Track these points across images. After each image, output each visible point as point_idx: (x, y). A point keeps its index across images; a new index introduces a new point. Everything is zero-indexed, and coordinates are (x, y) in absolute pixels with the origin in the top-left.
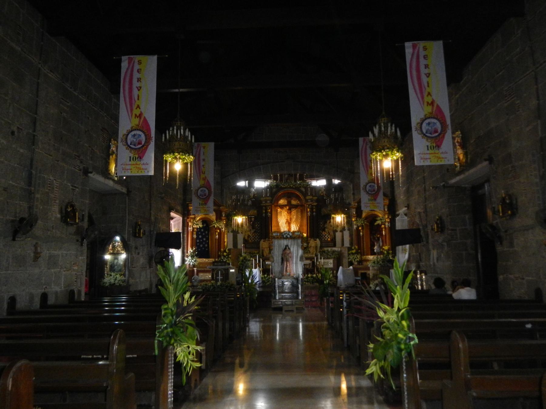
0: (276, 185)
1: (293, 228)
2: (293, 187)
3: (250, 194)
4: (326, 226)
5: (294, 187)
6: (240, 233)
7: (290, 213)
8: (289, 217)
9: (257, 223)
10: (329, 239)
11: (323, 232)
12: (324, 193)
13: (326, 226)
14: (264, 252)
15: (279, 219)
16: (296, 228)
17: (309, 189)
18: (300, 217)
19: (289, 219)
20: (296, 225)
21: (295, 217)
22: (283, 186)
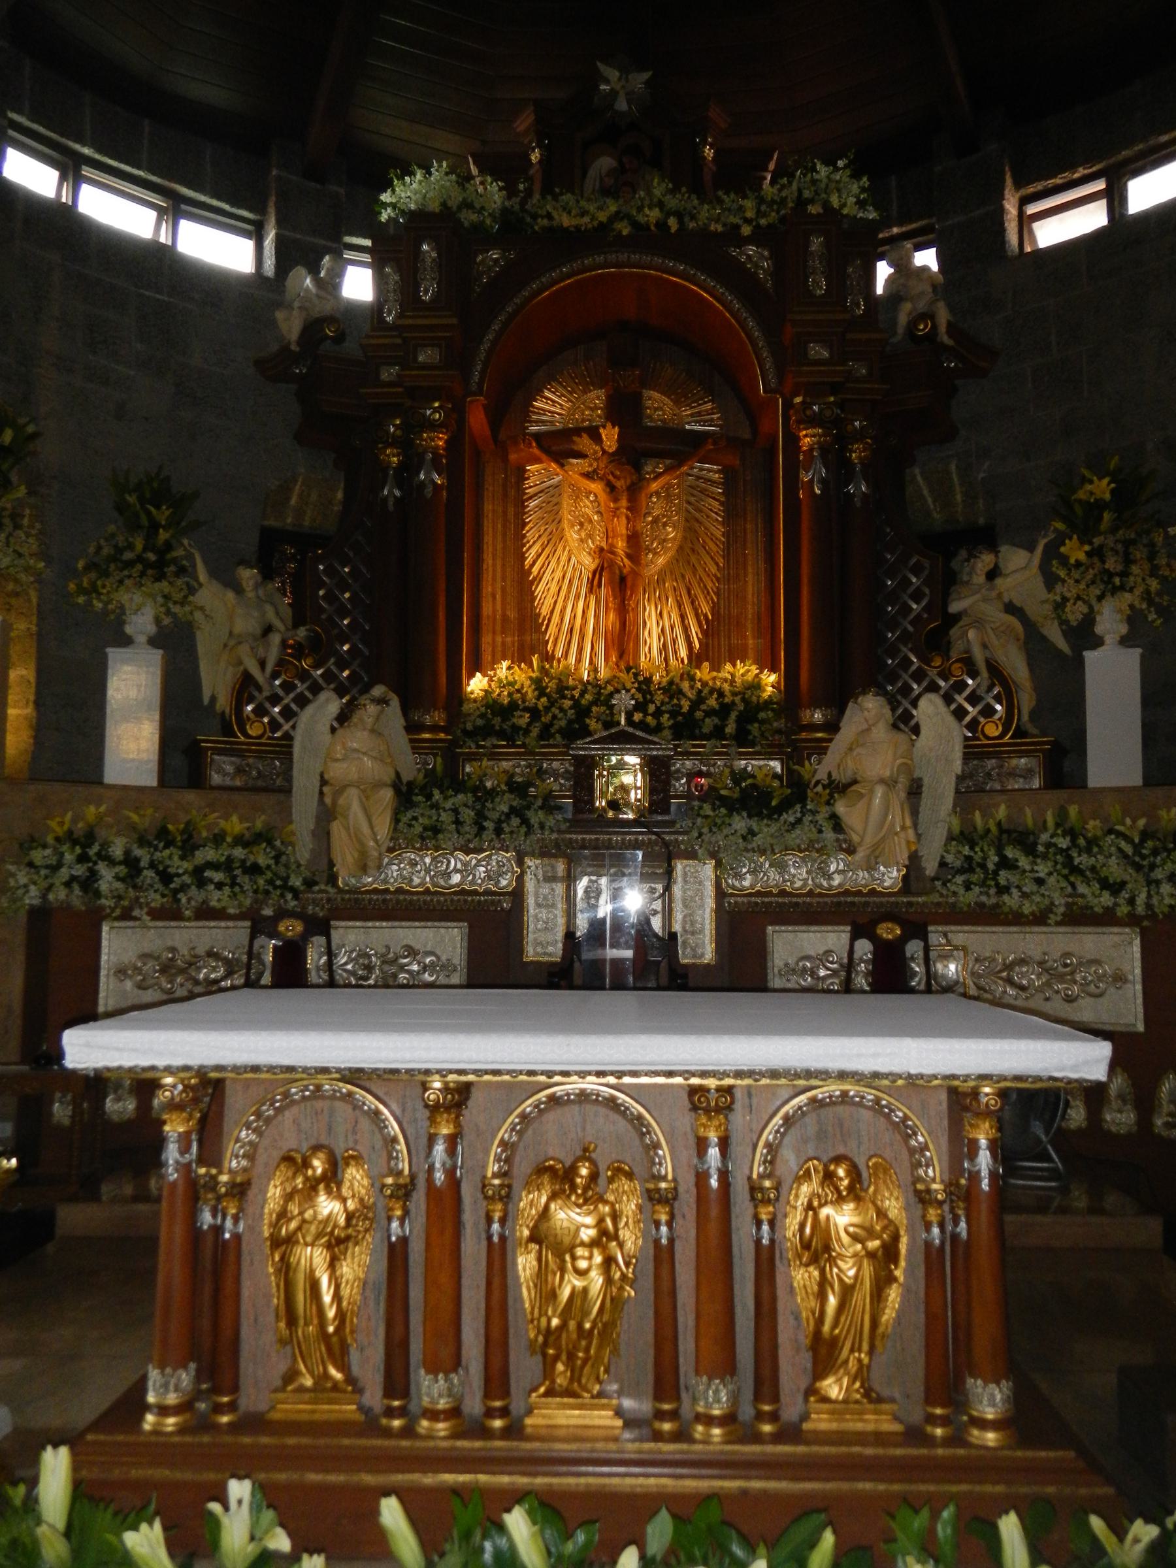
0: (505, 211)
1: (655, 632)
2: (662, 225)
3: (280, 315)
4: (955, 607)
5: (673, 222)
6: (142, 639)
7: (634, 491)
8: (621, 526)
9: (331, 571)
10: (993, 730)
11: (937, 662)
12: (943, 316)
13: (955, 607)
14: (336, 827)
15: (533, 551)
16: (686, 629)
17: (816, 243)
18: (718, 532)
19: (621, 545)
20: (680, 605)
21: (671, 533)
22: (566, 221)
